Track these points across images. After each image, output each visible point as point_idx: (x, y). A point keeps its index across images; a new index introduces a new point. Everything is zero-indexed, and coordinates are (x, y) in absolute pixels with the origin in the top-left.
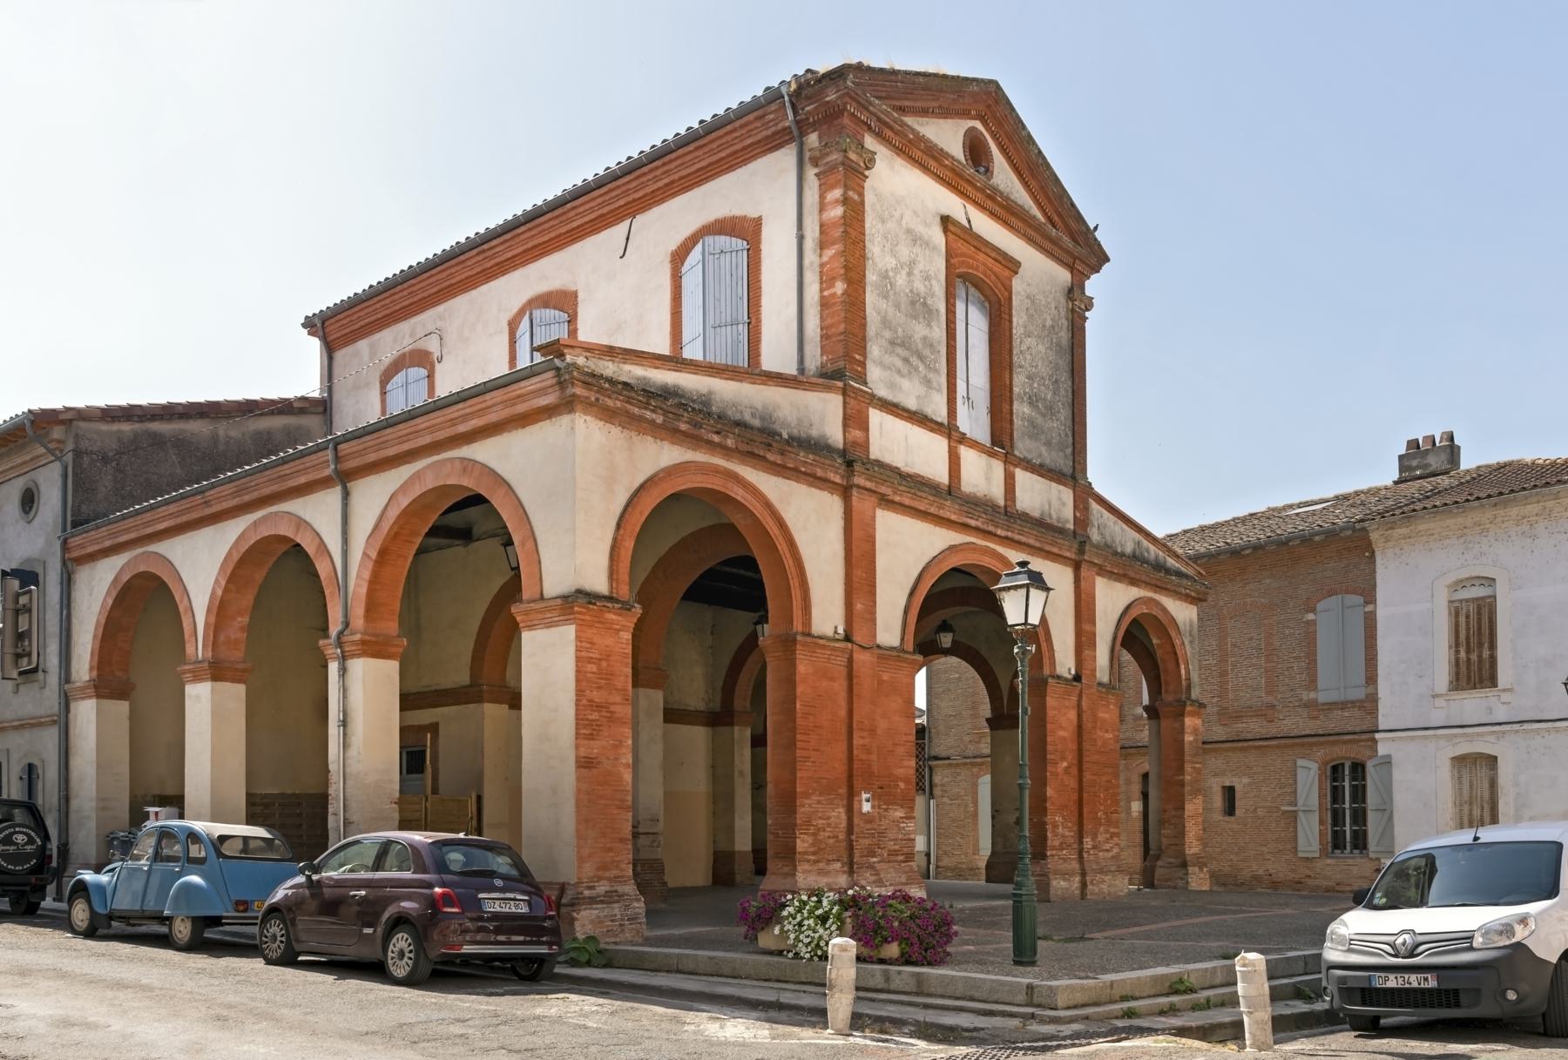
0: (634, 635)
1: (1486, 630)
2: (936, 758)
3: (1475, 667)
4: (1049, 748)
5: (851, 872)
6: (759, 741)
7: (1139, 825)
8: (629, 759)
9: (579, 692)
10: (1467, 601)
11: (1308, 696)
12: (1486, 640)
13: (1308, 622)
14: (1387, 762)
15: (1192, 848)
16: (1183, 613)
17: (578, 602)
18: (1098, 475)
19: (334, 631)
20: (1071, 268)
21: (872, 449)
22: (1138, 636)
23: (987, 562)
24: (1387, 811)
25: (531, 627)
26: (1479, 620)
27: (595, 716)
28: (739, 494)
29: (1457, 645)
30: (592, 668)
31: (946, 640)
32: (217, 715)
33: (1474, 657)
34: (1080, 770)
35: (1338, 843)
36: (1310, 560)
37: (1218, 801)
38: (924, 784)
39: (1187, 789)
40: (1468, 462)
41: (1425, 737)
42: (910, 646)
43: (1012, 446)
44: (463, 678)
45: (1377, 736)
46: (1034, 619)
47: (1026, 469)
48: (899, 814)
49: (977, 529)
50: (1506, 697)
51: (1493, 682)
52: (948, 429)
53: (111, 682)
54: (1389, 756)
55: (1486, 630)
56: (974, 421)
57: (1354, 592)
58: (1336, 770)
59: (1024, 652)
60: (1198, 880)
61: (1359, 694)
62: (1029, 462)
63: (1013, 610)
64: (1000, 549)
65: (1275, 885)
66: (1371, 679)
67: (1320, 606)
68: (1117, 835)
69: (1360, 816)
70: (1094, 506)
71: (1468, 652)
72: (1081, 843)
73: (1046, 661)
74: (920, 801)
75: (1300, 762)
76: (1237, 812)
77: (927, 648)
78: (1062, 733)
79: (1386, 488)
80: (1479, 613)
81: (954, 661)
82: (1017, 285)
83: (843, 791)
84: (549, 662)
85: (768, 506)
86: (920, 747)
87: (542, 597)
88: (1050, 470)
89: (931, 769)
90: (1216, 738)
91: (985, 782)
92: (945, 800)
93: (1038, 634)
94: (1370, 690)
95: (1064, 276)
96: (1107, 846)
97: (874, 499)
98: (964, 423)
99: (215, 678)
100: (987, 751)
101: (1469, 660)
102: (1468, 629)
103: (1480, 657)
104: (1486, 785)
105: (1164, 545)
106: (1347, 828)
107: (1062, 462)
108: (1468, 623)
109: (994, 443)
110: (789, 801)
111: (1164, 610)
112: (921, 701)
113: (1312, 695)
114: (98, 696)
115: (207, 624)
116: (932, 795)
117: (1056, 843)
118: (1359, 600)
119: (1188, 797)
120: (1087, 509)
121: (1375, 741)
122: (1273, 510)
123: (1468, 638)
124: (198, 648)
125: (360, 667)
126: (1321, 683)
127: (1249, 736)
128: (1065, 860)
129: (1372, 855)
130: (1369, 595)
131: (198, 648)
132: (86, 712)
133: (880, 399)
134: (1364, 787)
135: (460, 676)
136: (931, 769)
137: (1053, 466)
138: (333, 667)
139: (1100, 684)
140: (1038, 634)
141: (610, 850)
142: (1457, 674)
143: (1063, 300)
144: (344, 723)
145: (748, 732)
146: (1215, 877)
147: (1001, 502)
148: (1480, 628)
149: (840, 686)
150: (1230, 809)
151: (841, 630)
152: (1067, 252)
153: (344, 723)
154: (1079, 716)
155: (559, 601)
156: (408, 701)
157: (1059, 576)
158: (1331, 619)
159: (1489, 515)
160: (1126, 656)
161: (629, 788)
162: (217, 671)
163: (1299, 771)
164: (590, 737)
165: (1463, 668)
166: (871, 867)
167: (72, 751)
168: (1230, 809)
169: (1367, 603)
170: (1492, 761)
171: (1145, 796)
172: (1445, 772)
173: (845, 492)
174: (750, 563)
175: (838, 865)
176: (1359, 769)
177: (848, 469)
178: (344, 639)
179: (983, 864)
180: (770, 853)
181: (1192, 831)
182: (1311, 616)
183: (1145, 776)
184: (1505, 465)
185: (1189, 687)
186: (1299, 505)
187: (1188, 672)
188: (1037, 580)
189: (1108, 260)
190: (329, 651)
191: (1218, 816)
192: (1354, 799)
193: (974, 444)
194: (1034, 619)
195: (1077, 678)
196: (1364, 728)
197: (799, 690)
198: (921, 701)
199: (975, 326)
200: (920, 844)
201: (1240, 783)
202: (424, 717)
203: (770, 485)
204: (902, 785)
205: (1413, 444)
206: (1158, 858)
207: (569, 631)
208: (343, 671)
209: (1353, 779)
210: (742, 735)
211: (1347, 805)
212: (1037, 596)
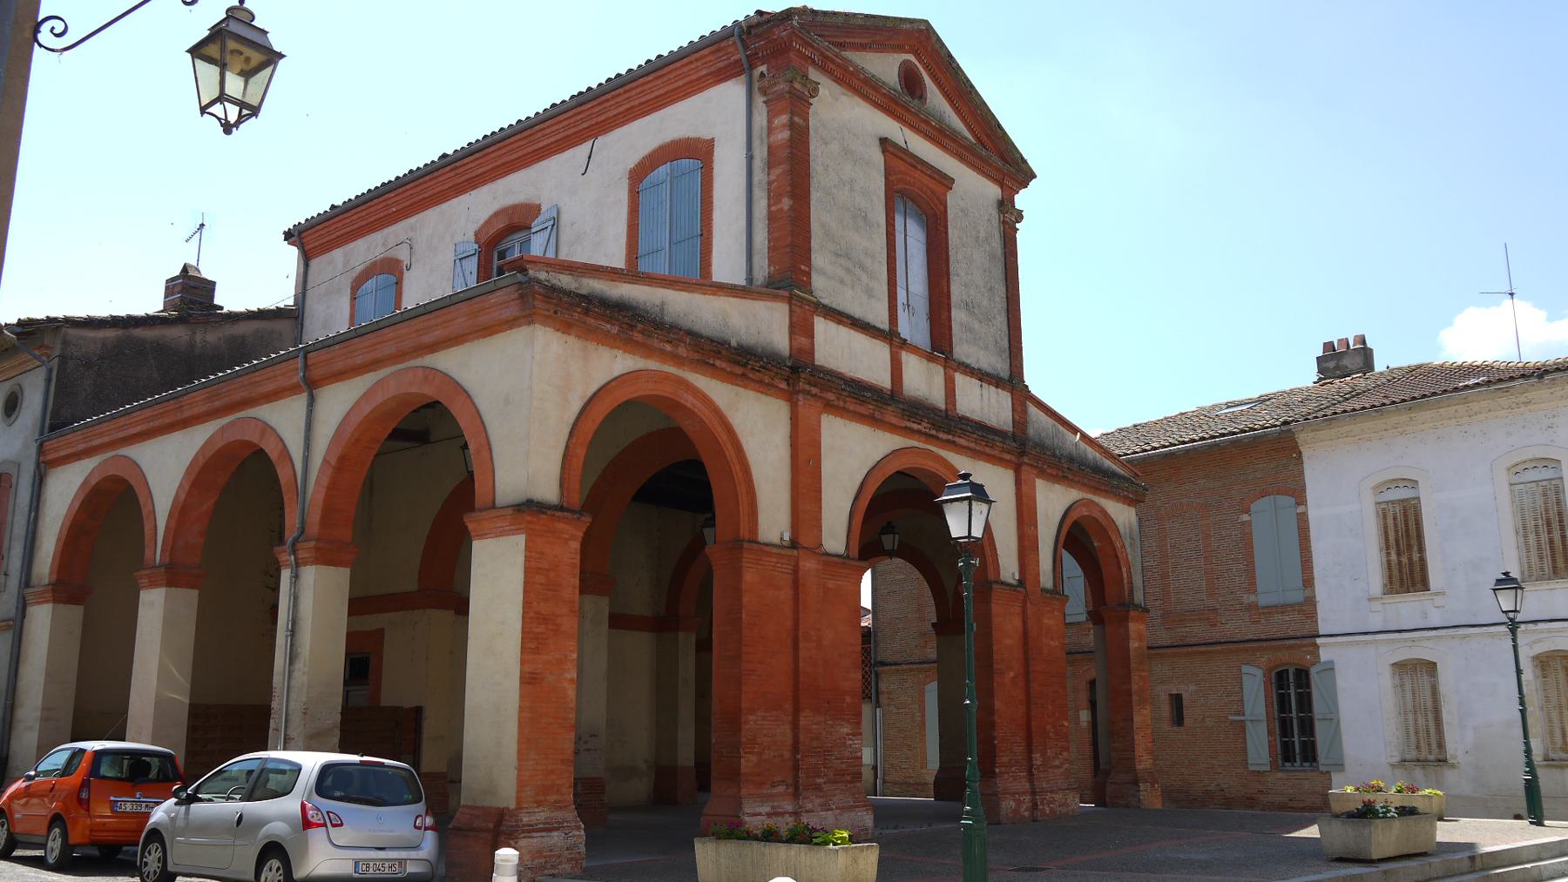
0: (582, 544)
1: (1413, 533)
2: (883, 664)
3: (1406, 570)
4: (995, 656)
5: (796, 795)
6: (704, 646)
7: (1087, 737)
8: (573, 674)
9: (527, 604)
10: (1393, 502)
11: (1249, 599)
12: (1414, 542)
13: (1243, 523)
14: (1330, 668)
15: (1144, 762)
16: (1122, 515)
17: (529, 509)
18: (1036, 379)
19: (290, 535)
20: (1001, 185)
21: (817, 355)
22: (1081, 538)
23: (930, 465)
24: (1333, 719)
25: (482, 536)
26: (1406, 521)
27: (542, 629)
28: (689, 400)
29: (1388, 548)
30: (540, 579)
31: (889, 541)
32: (169, 622)
33: (1405, 560)
34: (1027, 682)
35: (1287, 754)
36: (1244, 461)
37: (1166, 709)
38: (870, 692)
39: (1135, 698)
40: (1379, 366)
41: (1366, 643)
42: (855, 552)
43: (951, 352)
44: (411, 585)
45: (1319, 641)
46: (977, 532)
47: (965, 373)
48: (846, 730)
49: (919, 432)
50: (1439, 600)
51: (1425, 586)
52: (890, 336)
53: (69, 586)
54: (1332, 662)
55: (1413, 533)
56: (914, 327)
57: (1285, 493)
58: (1281, 677)
59: (967, 564)
60: (1151, 797)
61: (1297, 596)
62: (967, 366)
63: (957, 527)
64: (943, 453)
65: (1229, 803)
66: (1308, 582)
67: (1253, 507)
68: (1067, 749)
69: (1308, 727)
70: (1032, 409)
71: (1399, 554)
72: (1030, 759)
73: (991, 569)
74: (866, 709)
75: (1245, 669)
76: (1187, 721)
77: (868, 549)
78: (1008, 642)
79: (1308, 389)
80: (1405, 515)
81: (898, 561)
82: (952, 200)
83: (788, 706)
84: (498, 573)
85: (717, 412)
86: (866, 652)
87: (493, 506)
88: (988, 375)
89: (877, 675)
90: (1160, 643)
91: (932, 692)
92: (892, 708)
93: (982, 547)
94: (1308, 593)
95: (994, 191)
96: (1057, 763)
97: (819, 405)
98: (904, 330)
99: (170, 583)
100: (934, 656)
101: (1400, 563)
102: (1396, 531)
103: (1410, 559)
104: (1428, 693)
105: (1100, 446)
106: (1296, 739)
107: (1001, 367)
108: (1396, 526)
109: (933, 348)
110: (734, 720)
111: (1103, 511)
112: (866, 601)
113: (1252, 598)
114: (56, 600)
115: (167, 527)
116: (878, 704)
117: (1005, 759)
118: (1292, 500)
119: (1136, 708)
120: (1025, 411)
121: (1316, 646)
122: (1203, 409)
123: (1397, 541)
124: (157, 552)
125: (311, 575)
126: (1260, 586)
127: (1194, 641)
128: (1015, 779)
129: (1322, 768)
130: (1299, 495)
131: (157, 552)
132: (41, 618)
133: (825, 306)
134: (1309, 695)
135: (409, 583)
136: (877, 675)
137: (989, 370)
138: (286, 574)
139: (1044, 590)
140: (982, 547)
141: (552, 772)
142: (1390, 577)
143: (995, 213)
144: (293, 632)
145: (693, 638)
146: (1170, 795)
147: (943, 407)
148: (1407, 530)
149: (785, 594)
150: (1178, 718)
151: (787, 537)
152: (998, 169)
153: (293, 632)
154: (1025, 623)
155: (510, 511)
156: (357, 606)
157: (997, 480)
158: (1266, 516)
159: (1404, 418)
160: (1068, 560)
161: (572, 705)
162: (173, 576)
163: (1245, 678)
164: (536, 651)
165: (1395, 572)
166: (818, 788)
167: (22, 658)
168: (1178, 718)
169: (1298, 504)
170: (1431, 667)
171: (1093, 705)
172: (1387, 680)
173: (791, 397)
174: (697, 466)
175: (781, 789)
176: (1303, 676)
177: (795, 377)
178: (299, 546)
179: (931, 779)
180: (714, 774)
181: (1141, 741)
182: (1245, 517)
183: (1092, 683)
184: (1419, 367)
185: (1131, 591)
186: (1228, 406)
187: (1130, 576)
188: (979, 493)
189: (1034, 176)
190: (283, 557)
191: (1166, 726)
192: (1301, 708)
193: (915, 350)
194: (977, 532)
195: (1021, 582)
196: (1305, 633)
197: (745, 600)
198: (866, 601)
199: (913, 239)
200: (867, 756)
201: (1188, 691)
202: (370, 622)
203: (719, 392)
204: (848, 699)
205: (1328, 346)
206: (1109, 778)
207: (519, 541)
208: (296, 577)
209: (1298, 686)
210: (687, 642)
211: (1294, 714)
212: (979, 509)
